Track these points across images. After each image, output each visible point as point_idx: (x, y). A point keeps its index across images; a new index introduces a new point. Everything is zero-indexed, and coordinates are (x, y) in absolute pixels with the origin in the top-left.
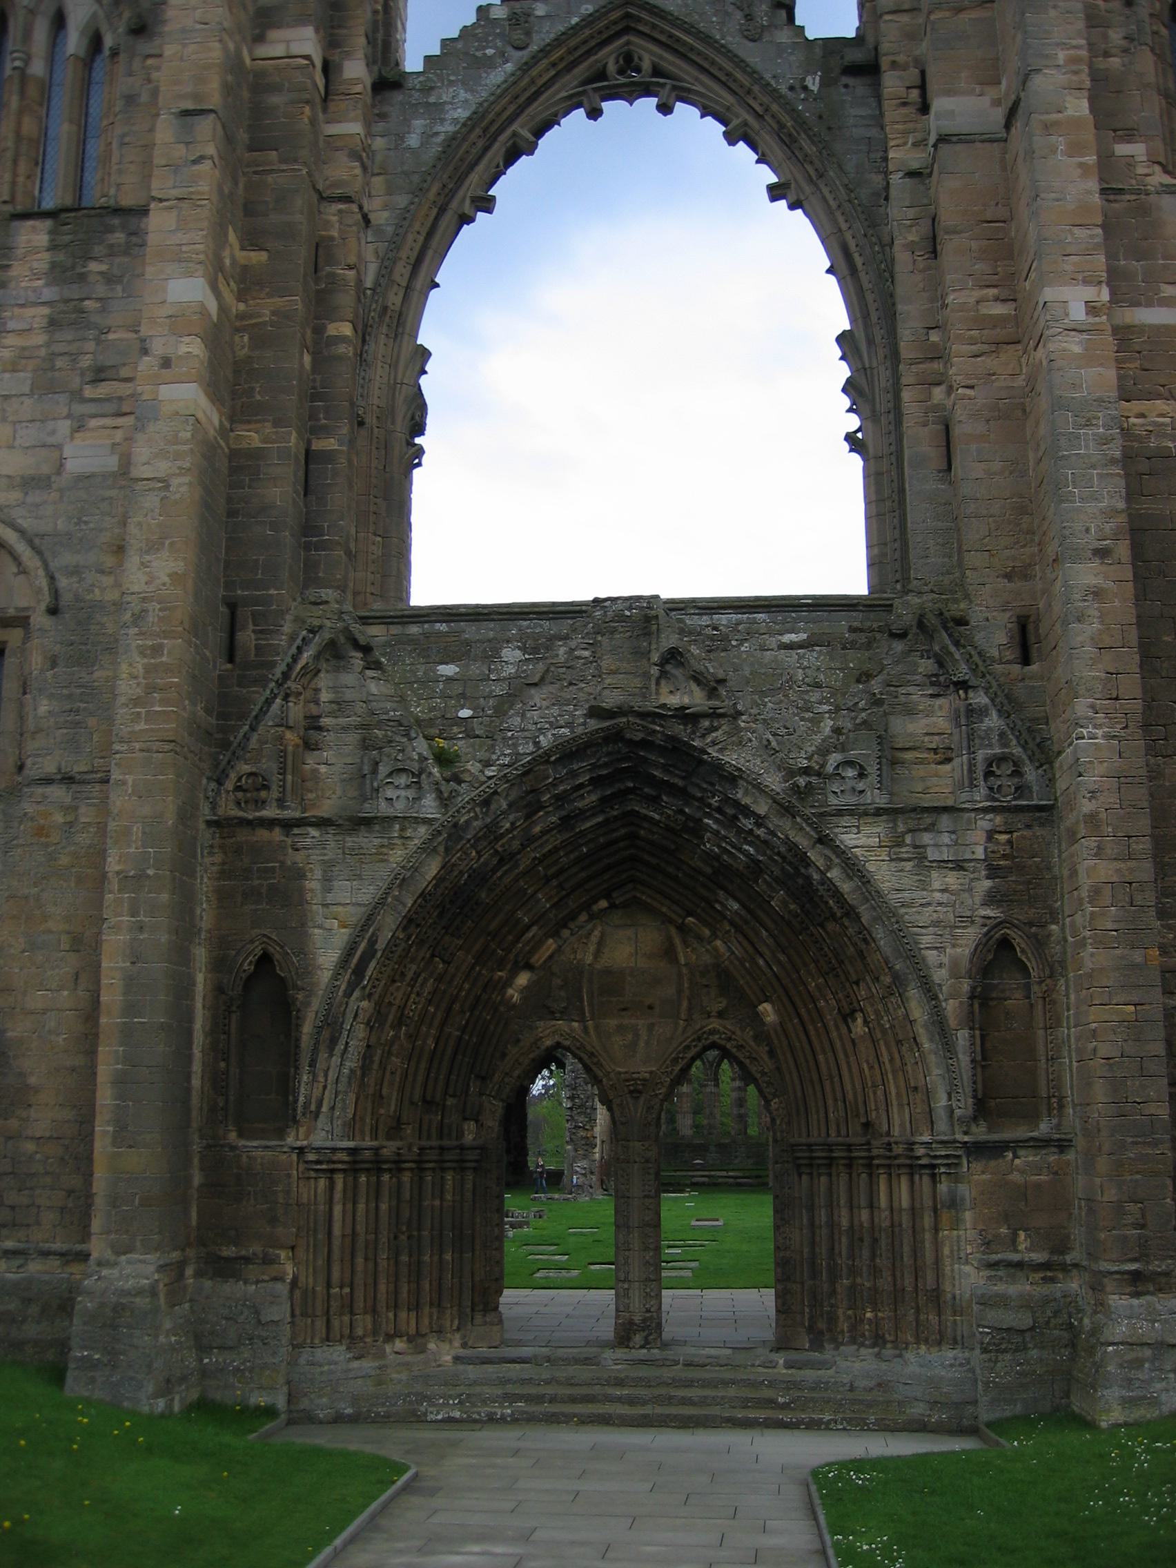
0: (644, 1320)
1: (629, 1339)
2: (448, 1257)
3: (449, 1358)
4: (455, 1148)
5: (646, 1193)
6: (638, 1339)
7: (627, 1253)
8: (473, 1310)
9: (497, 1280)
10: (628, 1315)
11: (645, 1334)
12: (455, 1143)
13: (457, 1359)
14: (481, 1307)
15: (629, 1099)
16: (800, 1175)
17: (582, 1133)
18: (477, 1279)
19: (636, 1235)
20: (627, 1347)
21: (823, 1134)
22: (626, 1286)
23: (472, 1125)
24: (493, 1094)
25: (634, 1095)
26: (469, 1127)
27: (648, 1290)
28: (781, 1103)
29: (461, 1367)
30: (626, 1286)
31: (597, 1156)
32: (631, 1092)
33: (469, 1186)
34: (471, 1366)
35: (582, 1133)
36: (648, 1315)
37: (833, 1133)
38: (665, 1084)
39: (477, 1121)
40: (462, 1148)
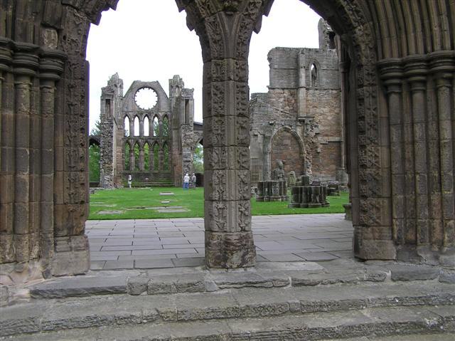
0: (241, 239)
1: (226, 259)
2: (25, 176)
3: (25, 292)
4: (32, 51)
5: (241, 111)
6: (236, 258)
7: (221, 172)
8: (55, 236)
9: (82, 202)
10: (223, 234)
11: (241, 253)
12: (30, 45)
13: (36, 294)
14: (65, 232)
15: (224, 16)
16: (387, 96)
17: (107, 165)
18: (60, 201)
19: (231, 153)
20: (224, 267)
21: (421, 49)
22: (221, 205)
23: (53, 34)
24: (77, 5)
25: (229, 13)
26: (49, 35)
27: (243, 209)
28: (366, 29)
29: (40, 303)
30: (221, 205)
31: (113, 174)
32: (225, 9)
33: (50, 99)
34: (54, 300)
35: (107, 165)
36: (244, 234)
37: (437, 47)
38: (257, 5)
39: (59, 31)
40: (42, 56)
